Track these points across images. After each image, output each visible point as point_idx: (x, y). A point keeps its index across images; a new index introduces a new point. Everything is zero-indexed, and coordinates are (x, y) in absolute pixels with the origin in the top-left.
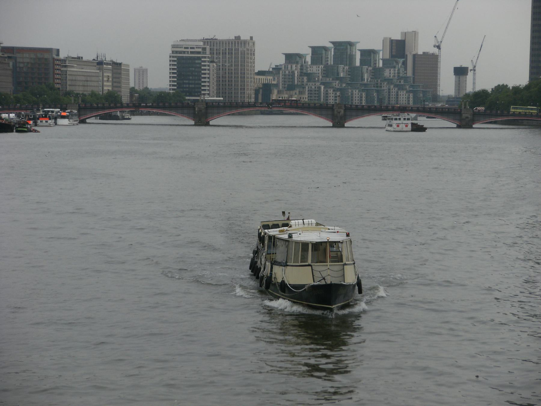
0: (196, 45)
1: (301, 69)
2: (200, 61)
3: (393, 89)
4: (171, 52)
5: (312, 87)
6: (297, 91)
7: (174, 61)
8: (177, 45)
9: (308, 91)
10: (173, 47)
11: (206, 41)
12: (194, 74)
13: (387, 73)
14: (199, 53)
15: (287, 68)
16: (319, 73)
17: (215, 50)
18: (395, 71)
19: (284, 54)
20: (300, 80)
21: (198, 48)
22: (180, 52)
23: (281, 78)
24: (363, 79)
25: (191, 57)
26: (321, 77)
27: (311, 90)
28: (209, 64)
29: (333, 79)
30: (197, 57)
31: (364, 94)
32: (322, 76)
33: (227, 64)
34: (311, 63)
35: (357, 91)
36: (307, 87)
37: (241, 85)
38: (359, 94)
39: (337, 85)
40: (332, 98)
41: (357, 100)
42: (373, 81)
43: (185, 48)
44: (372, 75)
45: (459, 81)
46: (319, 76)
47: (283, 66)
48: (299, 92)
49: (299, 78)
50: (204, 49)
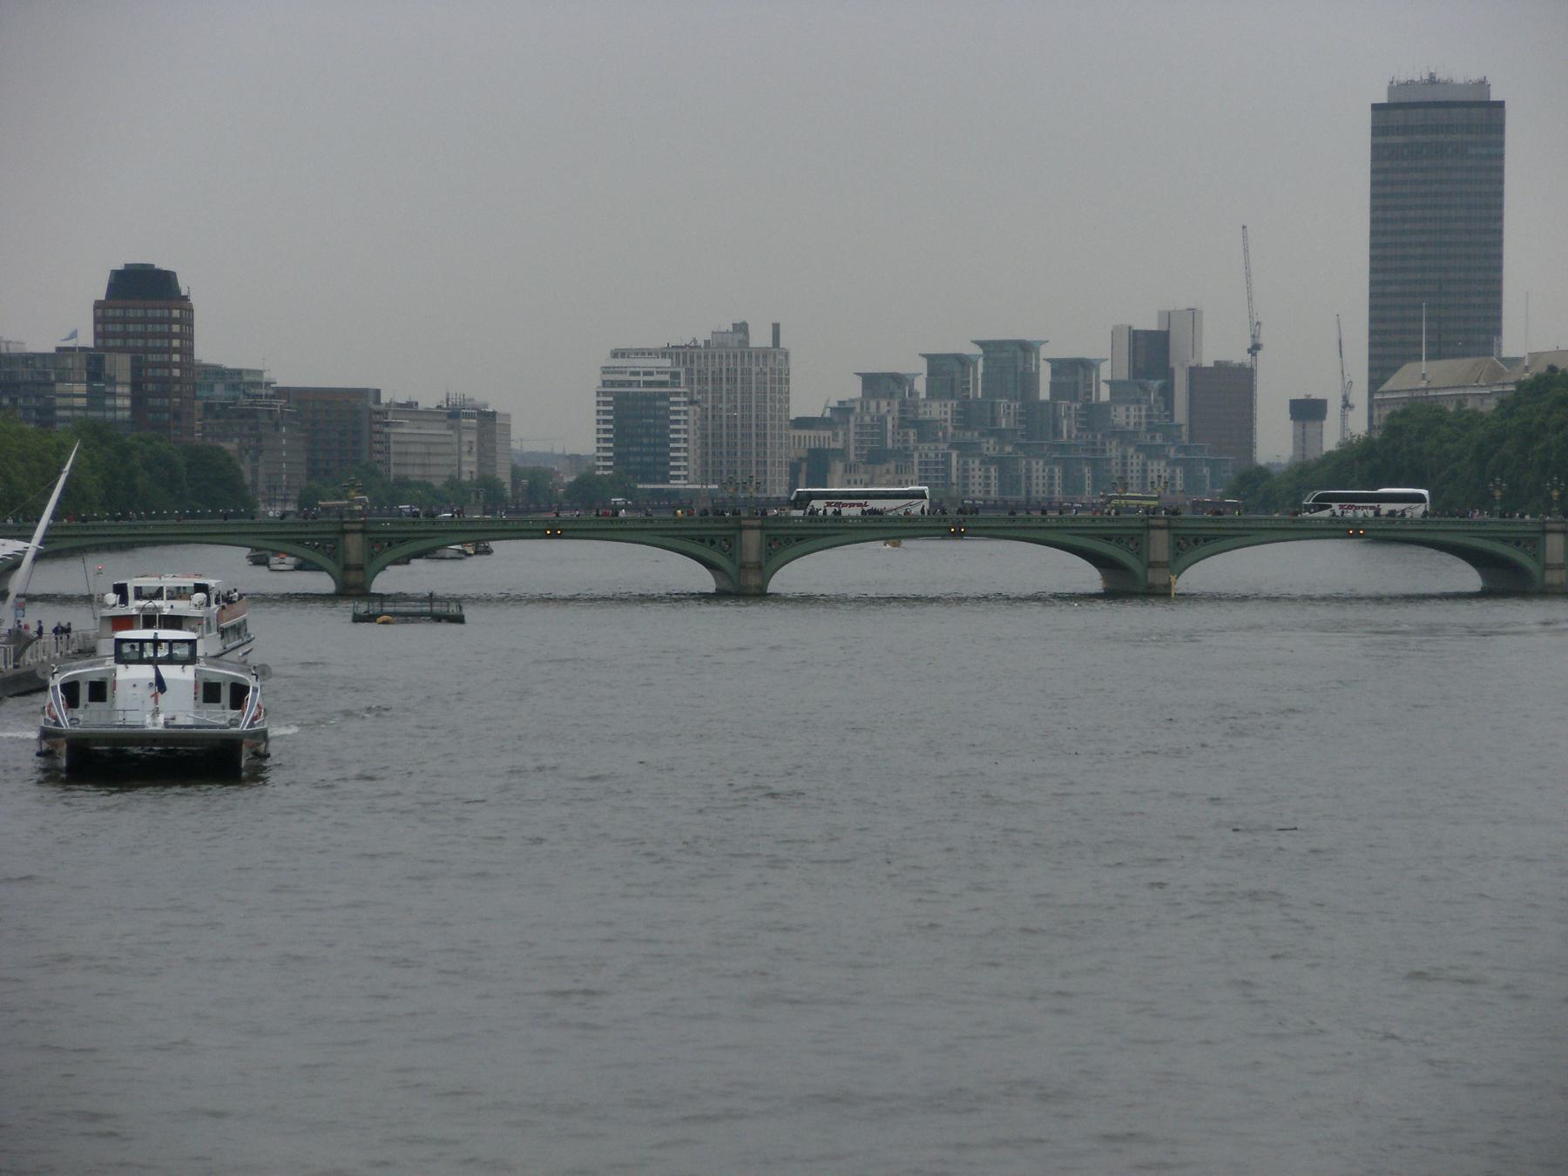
0: (657, 368)
1: (902, 411)
2: (665, 404)
3: (1135, 457)
4: (600, 384)
5: (930, 455)
6: (892, 466)
7: (606, 403)
8: (614, 367)
9: (920, 463)
10: (604, 373)
11: (674, 351)
12: (653, 431)
13: (1124, 416)
14: (662, 384)
15: (868, 408)
16: (946, 420)
17: (695, 372)
18: (1140, 410)
19: (858, 374)
20: (900, 437)
21: (662, 373)
22: (621, 384)
23: (852, 435)
24: (1057, 432)
25: (645, 393)
26: (950, 429)
27: (927, 463)
28: (686, 408)
29: (982, 435)
30: (659, 393)
31: (1057, 470)
32: (955, 428)
33: (724, 406)
34: (927, 394)
35: (1041, 463)
36: (916, 455)
37: (757, 455)
38: (1047, 470)
39: (991, 448)
40: (977, 480)
41: (1041, 485)
42: (1084, 436)
43: (632, 374)
44: (1083, 423)
45: (1304, 434)
46: (946, 427)
47: (858, 406)
48: (897, 466)
49: (896, 433)
50: (675, 375)
